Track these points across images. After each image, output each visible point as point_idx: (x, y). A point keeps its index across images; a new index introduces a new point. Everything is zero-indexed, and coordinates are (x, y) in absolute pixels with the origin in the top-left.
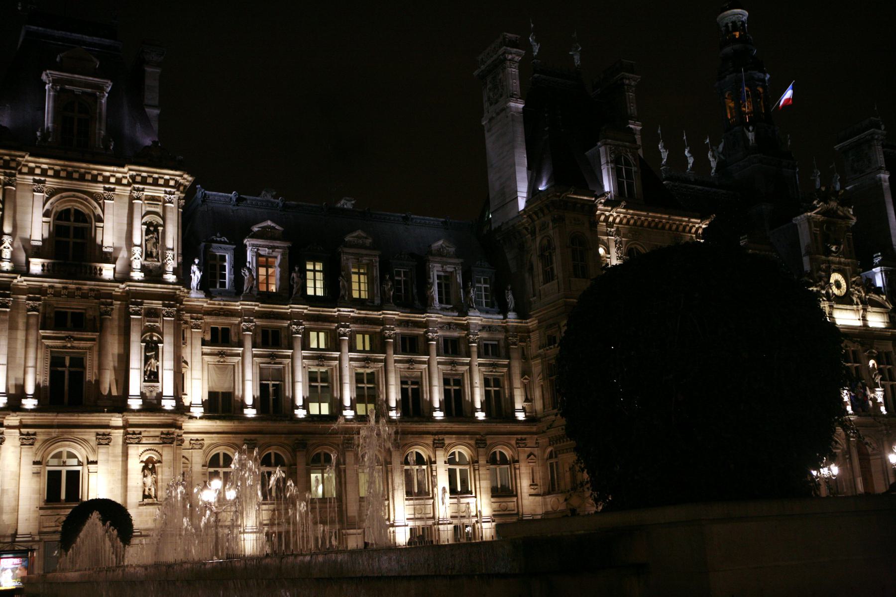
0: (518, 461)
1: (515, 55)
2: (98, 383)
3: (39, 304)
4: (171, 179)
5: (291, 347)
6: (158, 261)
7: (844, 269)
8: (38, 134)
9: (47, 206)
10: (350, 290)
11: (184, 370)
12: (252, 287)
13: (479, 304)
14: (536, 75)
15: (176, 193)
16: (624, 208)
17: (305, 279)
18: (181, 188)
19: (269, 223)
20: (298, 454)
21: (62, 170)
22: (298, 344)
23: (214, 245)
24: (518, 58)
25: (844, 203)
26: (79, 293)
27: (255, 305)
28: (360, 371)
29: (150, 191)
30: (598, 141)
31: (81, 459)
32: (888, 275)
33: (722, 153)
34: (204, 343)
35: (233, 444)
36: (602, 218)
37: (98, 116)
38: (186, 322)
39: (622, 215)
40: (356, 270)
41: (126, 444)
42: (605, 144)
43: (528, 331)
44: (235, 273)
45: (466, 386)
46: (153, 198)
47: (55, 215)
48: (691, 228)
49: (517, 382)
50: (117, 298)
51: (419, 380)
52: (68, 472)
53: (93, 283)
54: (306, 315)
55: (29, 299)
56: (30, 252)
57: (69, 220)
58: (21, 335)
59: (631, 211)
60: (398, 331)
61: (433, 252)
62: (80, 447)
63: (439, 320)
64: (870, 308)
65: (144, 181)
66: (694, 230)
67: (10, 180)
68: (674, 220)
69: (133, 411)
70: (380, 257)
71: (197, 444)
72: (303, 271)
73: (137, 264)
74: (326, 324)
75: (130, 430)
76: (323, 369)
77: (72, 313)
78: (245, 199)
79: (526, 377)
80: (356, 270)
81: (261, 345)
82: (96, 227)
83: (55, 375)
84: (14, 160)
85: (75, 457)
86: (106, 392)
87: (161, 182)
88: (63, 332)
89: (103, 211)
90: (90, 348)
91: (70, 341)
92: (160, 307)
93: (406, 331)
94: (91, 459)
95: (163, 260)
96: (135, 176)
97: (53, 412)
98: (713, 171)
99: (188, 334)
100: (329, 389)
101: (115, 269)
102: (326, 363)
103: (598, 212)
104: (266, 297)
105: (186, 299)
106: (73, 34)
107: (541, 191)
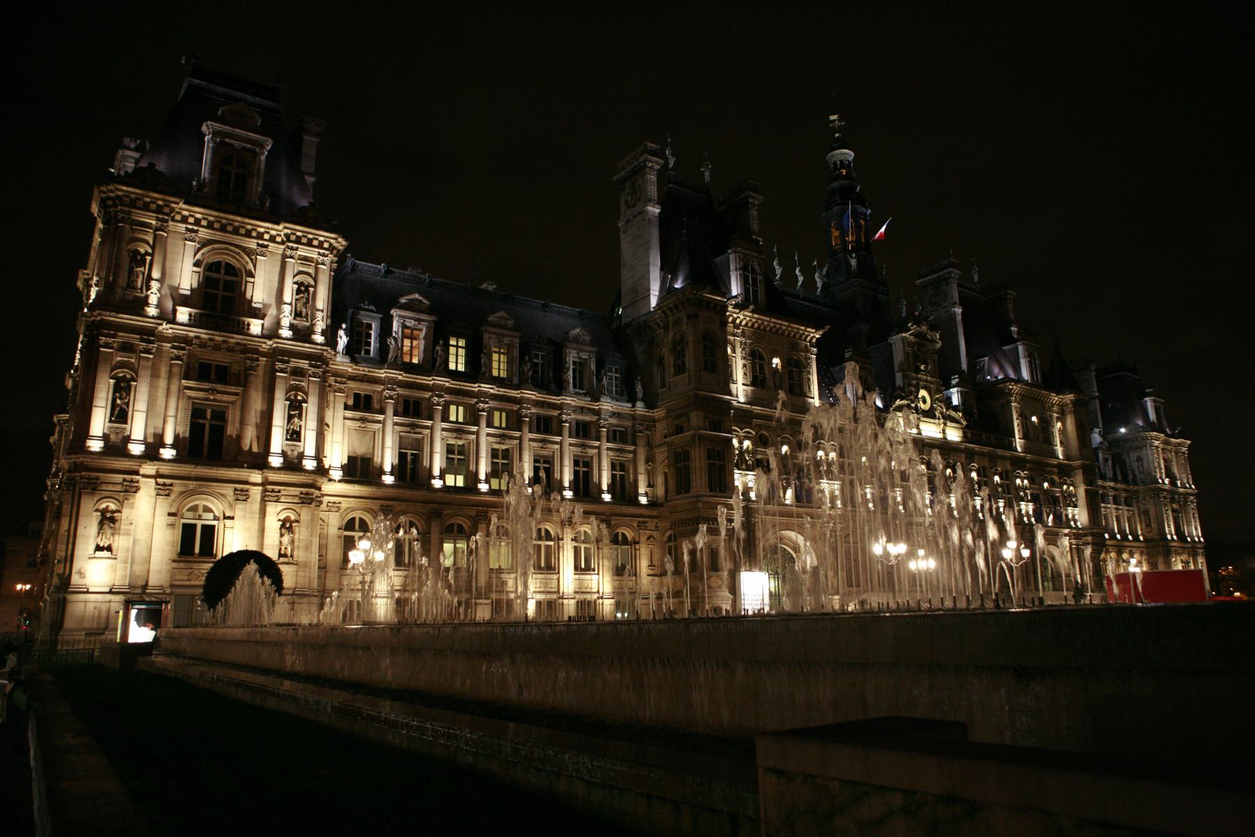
0: (638, 543)
1: (654, 163)
2: (239, 438)
3: (184, 354)
4: (325, 241)
5: (431, 418)
6: (307, 321)
7: (930, 387)
8: (194, 183)
9: (199, 256)
11: (326, 432)
12: (396, 357)
13: (610, 392)
14: (671, 185)
18: (335, 252)
19: (417, 296)
20: (433, 524)
21: (216, 221)
22: (438, 416)
23: (363, 313)
24: (657, 167)
25: (933, 328)
27: (399, 374)
29: (303, 251)
30: (729, 249)
31: (217, 514)
32: (963, 395)
33: (825, 276)
34: (346, 407)
36: (731, 319)
37: (256, 172)
38: (330, 386)
39: (748, 319)
40: (497, 350)
41: (264, 501)
42: (736, 252)
43: (654, 421)
44: (380, 342)
46: (306, 259)
47: (205, 266)
48: (806, 337)
49: (642, 468)
50: (264, 354)
51: (551, 459)
52: (203, 526)
53: (240, 337)
54: (448, 388)
55: (173, 347)
56: (177, 300)
57: (219, 272)
58: (162, 383)
59: (756, 316)
60: (534, 410)
61: (571, 339)
62: (216, 501)
63: (573, 403)
65: (298, 241)
66: (808, 339)
67: (162, 225)
68: (792, 327)
69: (274, 469)
70: (520, 338)
71: (335, 507)
72: (447, 346)
73: (286, 321)
75: (270, 487)
76: (460, 443)
77: (217, 366)
78: (393, 272)
80: (497, 350)
82: (246, 282)
83: (196, 428)
84: (168, 206)
85: (210, 511)
86: (246, 448)
89: (255, 267)
90: (233, 403)
91: (212, 394)
92: (306, 366)
93: (542, 412)
94: (228, 514)
95: (312, 321)
97: (193, 464)
98: (819, 290)
99: (331, 397)
100: (464, 462)
101: (263, 325)
102: (464, 436)
103: (728, 313)
104: (409, 368)
105: (331, 362)
106: (236, 93)
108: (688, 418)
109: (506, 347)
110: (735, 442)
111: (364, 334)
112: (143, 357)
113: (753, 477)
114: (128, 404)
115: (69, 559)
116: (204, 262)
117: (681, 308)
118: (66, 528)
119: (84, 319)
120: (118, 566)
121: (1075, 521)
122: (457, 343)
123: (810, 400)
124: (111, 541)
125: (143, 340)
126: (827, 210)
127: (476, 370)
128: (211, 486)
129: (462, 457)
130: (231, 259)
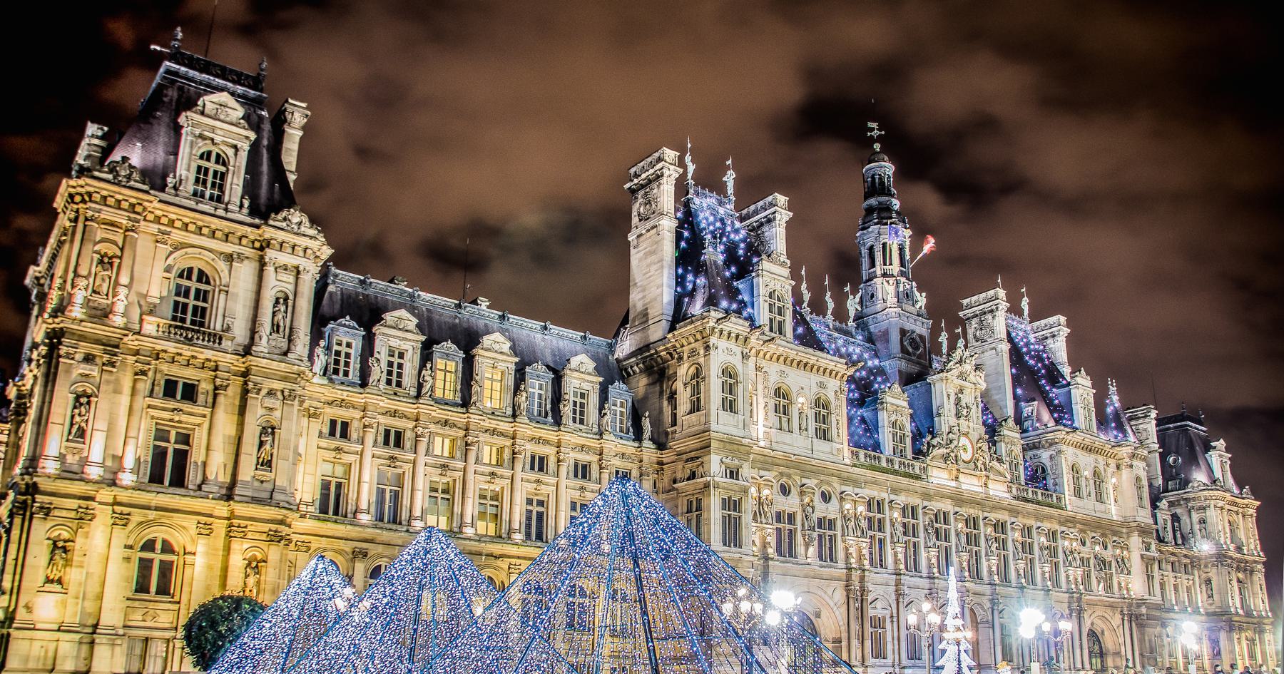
35: (342, 550)
41: (229, 536)
62: (178, 535)
75: (236, 522)
76: (445, 480)
77: (185, 384)
90: (199, 425)
102: (449, 473)
113: (771, 531)
114: (87, 420)
115: (15, 591)
116: (175, 268)
118: (14, 557)
120: (69, 601)
121: (1128, 590)
124: (62, 574)
126: (863, 229)
128: (172, 517)
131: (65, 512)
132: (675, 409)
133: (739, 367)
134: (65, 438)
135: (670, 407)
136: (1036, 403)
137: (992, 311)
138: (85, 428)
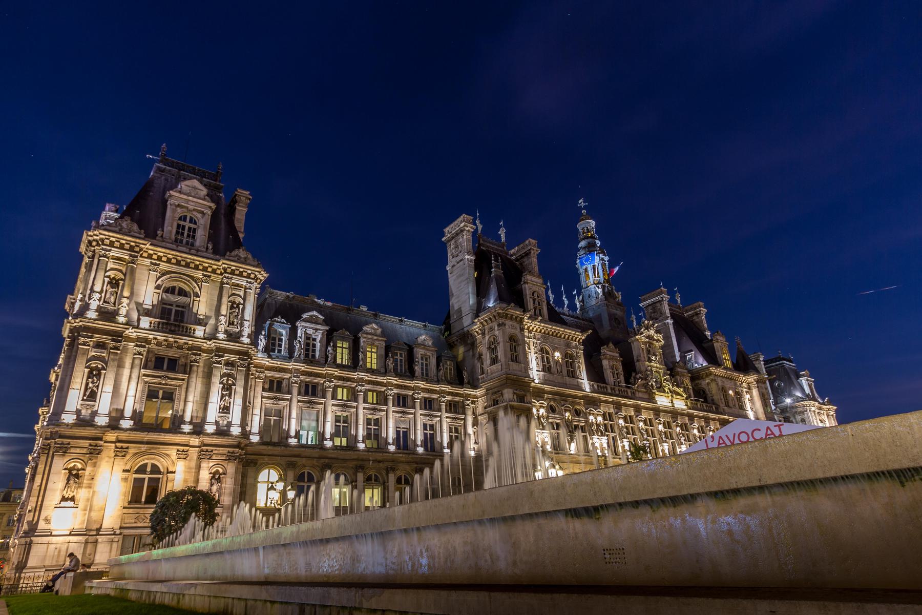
3: (144, 351)
5: (324, 396)
6: (238, 328)
9: (159, 282)
10: (365, 361)
12: (300, 354)
15: (255, 283)
16: (538, 322)
17: (335, 351)
18: (258, 281)
19: (315, 313)
26: (176, 345)
27: (302, 366)
28: (370, 417)
33: (581, 301)
36: (526, 327)
39: (537, 327)
41: (200, 458)
45: (438, 431)
46: (238, 285)
50: (204, 351)
54: (336, 376)
55: (137, 346)
56: (141, 312)
59: (543, 325)
60: (395, 391)
62: (163, 460)
64: (675, 396)
65: (233, 273)
66: (577, 340)
68: (566, 332)
72: (335, 347)
73: (222, 328)
74: (349, 383)
76: (345, 414)
79: (475, 427)
80: (370, 350)
81: (304, 394)
84: (138, 246)
87: (245, 274)
88: (160, 372)
89: (200, 290)
90: (180, 386)
91: (165, 379)
92: (236, 360)
94: (170, 470)
95: (241, 328)
96: (227, 268)
101: (205, 330)
107: (489, 307)
108: (502, 393)
109: (376, 348)
110: (534, 411)
111: (277, 340)
112: (112, 352)
113: (547, 434)
114: (98, 386)
115: (38, 509)
117: (493, 319)
118: (39, 484)
119: (69, 324)
122: (343, 345)
123: (581, 381)
124: (75, 493)
125: (113, 340)
127: (355, 363)
129: (346, 425)
130: (183, 284)
131: (78, 449)
132: (482, 364)
133: (519, 336)
134: (81, 399)
135: (479, 364)
136: (693, 352)
137: (659, 301)
138: (96, 391)
